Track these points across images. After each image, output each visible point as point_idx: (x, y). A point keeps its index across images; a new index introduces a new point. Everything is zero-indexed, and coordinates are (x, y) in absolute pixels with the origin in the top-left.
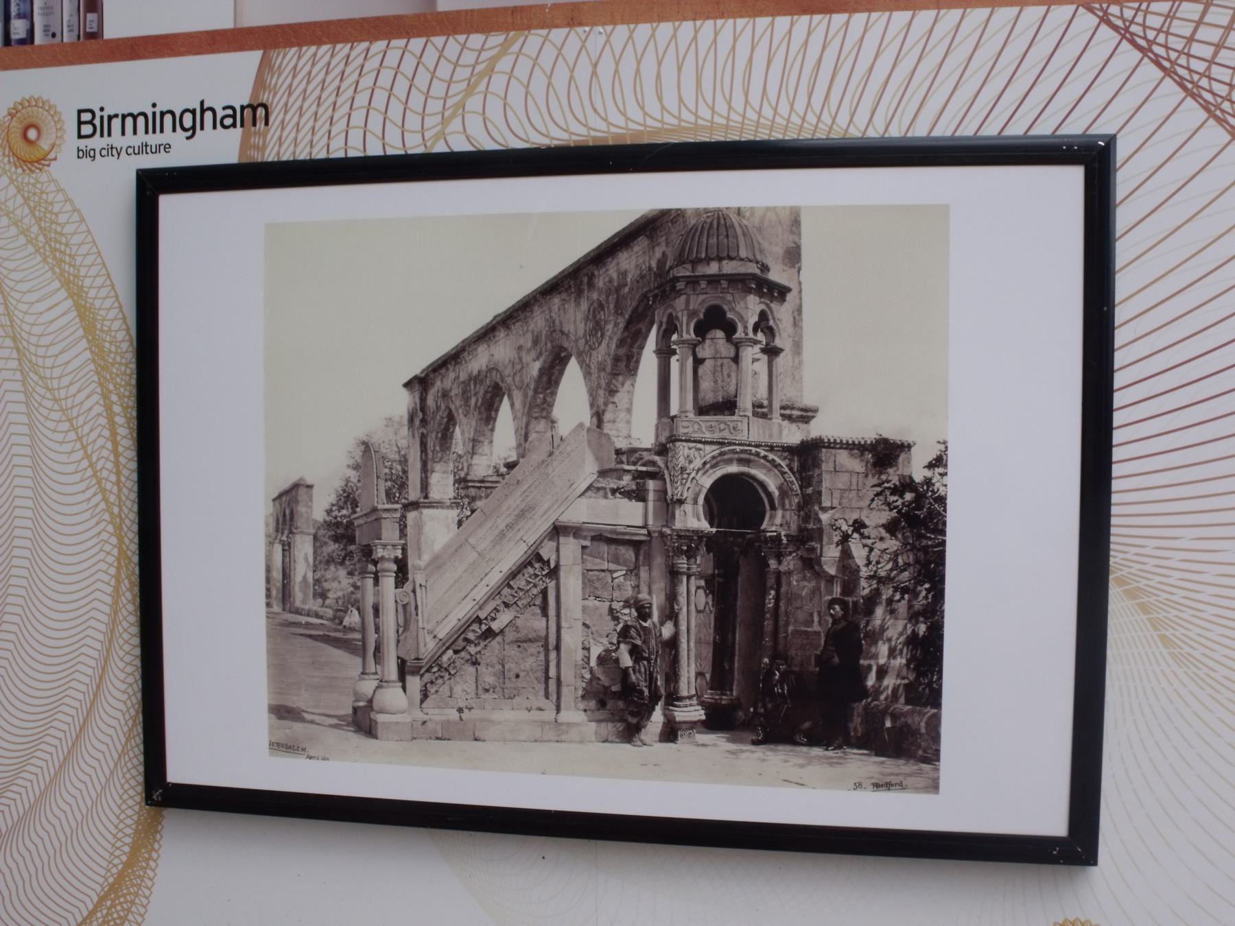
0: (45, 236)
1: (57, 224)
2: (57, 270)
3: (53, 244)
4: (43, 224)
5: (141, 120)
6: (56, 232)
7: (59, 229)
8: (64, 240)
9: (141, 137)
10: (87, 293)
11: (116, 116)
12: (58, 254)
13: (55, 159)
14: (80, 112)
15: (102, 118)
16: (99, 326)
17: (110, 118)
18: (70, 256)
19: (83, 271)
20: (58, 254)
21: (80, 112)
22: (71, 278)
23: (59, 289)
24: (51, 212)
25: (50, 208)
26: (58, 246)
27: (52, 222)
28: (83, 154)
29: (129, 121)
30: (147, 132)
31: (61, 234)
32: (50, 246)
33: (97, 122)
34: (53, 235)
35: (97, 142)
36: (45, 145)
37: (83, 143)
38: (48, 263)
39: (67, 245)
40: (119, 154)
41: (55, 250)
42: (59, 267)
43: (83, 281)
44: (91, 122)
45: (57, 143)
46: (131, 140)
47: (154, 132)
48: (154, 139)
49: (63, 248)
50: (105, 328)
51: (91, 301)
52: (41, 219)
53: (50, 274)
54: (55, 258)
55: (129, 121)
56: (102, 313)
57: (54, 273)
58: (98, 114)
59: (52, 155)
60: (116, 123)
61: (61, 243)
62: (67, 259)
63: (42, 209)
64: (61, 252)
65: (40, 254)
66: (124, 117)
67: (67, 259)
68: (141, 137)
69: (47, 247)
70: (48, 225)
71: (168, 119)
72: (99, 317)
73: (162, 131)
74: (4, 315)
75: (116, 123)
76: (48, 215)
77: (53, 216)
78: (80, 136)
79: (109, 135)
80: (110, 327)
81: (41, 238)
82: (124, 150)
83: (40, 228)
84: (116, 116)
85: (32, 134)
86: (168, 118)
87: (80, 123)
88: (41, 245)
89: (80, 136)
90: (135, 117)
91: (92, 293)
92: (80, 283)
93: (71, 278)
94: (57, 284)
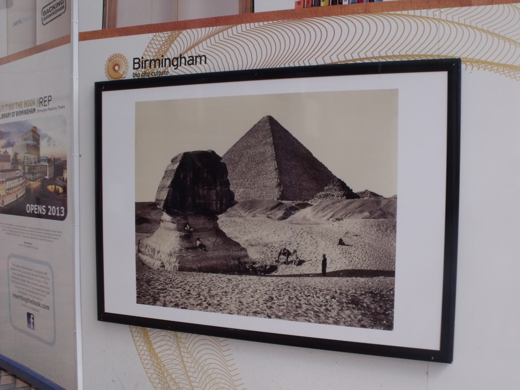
0: (164, 375)
1: (159, 379)
2: (159, 361)
3: (161, 371)
4: (165, 381)
6: (160, 376)
7: (159, 377)
8: (157, 372)
10: (147, 349)
12: (159, 367)
16: (142, 335)
18: (154, 366)
19: (149, 358)
20: (159, 367)
22: (153, 356)
23: (158, 353)
24: (162, 384)
25: (162, 386)
26: (159, 370)
27: (161, 380)
31: (158, 375)
32: (162, 371)
34: (161, 375)
38: (163, 364)
39: (155, 370)
41: (160, 369)
42: (158, 362)
43: (149, 354)
49: (157, 369)
50: (140, 334)
51: (145, 345)
52: (166, 383)
53: (162, 360)
54: (160, 366)
56: (141, 340)
57: (160, 360)
61: (158, 371)
62: (155, 364)
63: (165, 387)
64: (158, 368)
65: (166, 369)
67: (155, 364)
69: (163, 371)
70: (163, 380)
72: (142, 338)
74: (181, 347)
76: (163, 383)
77: (161, 382)
80: (138, 334)
81: (166, 375)
83: (166, 379)
88: (166, 372)
91: (145, 348)
92: (150, 353)
93: (153, 356)
94: (159, 355)
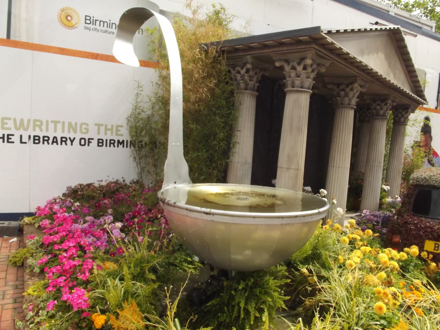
5: (106, 24)
9: (105, 28)
11: (98, 20)
13: (77, 27)
14: (86, 16)
15: (93, 20)
17: (96, 20)
21: (86, 16)
28: (86, 28)
29: (102, 23)
30: (107, 27)
33: (92, 20)
35: (91, 26)
36: (73, 22)
37: (87, 25)
40: (98, 31)
44: (90, 20)
45: (78, 23)
46: (101, 28)
47: (110, 28)
48: (110, 30)
55: (102, 23)
58: (92, 18)
59: (76, 26)
60: (98, 23)
66: (100, 21)
68: (105, 28)
71: (114, 25)
73: (112, 28)
75: (98, 23)
78: (86, 23)
79: (95, 25)
82: (100, 31)
84: (98, 20)
85: (69, 18)
86: (114, 25)
87: (86, 19)
89: (86, 23)
90: (104, 22)
